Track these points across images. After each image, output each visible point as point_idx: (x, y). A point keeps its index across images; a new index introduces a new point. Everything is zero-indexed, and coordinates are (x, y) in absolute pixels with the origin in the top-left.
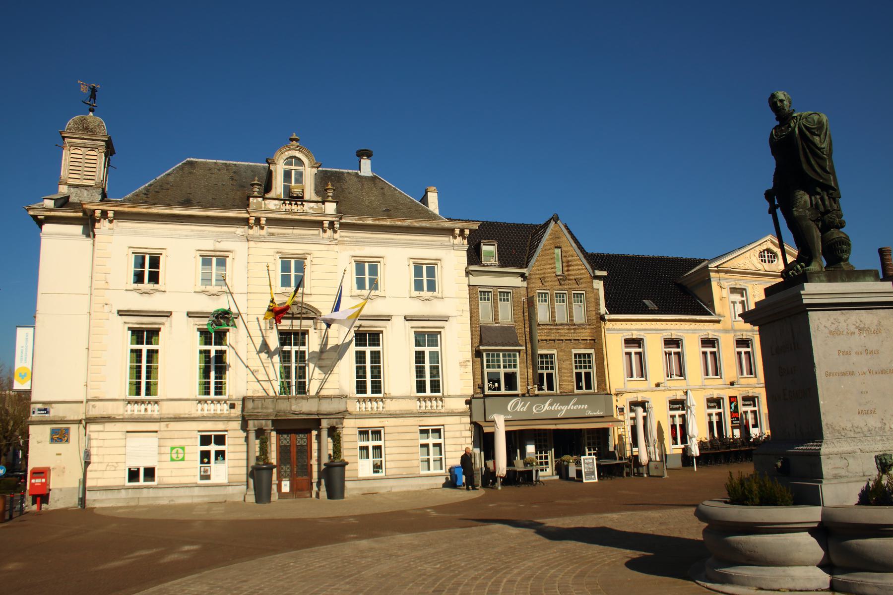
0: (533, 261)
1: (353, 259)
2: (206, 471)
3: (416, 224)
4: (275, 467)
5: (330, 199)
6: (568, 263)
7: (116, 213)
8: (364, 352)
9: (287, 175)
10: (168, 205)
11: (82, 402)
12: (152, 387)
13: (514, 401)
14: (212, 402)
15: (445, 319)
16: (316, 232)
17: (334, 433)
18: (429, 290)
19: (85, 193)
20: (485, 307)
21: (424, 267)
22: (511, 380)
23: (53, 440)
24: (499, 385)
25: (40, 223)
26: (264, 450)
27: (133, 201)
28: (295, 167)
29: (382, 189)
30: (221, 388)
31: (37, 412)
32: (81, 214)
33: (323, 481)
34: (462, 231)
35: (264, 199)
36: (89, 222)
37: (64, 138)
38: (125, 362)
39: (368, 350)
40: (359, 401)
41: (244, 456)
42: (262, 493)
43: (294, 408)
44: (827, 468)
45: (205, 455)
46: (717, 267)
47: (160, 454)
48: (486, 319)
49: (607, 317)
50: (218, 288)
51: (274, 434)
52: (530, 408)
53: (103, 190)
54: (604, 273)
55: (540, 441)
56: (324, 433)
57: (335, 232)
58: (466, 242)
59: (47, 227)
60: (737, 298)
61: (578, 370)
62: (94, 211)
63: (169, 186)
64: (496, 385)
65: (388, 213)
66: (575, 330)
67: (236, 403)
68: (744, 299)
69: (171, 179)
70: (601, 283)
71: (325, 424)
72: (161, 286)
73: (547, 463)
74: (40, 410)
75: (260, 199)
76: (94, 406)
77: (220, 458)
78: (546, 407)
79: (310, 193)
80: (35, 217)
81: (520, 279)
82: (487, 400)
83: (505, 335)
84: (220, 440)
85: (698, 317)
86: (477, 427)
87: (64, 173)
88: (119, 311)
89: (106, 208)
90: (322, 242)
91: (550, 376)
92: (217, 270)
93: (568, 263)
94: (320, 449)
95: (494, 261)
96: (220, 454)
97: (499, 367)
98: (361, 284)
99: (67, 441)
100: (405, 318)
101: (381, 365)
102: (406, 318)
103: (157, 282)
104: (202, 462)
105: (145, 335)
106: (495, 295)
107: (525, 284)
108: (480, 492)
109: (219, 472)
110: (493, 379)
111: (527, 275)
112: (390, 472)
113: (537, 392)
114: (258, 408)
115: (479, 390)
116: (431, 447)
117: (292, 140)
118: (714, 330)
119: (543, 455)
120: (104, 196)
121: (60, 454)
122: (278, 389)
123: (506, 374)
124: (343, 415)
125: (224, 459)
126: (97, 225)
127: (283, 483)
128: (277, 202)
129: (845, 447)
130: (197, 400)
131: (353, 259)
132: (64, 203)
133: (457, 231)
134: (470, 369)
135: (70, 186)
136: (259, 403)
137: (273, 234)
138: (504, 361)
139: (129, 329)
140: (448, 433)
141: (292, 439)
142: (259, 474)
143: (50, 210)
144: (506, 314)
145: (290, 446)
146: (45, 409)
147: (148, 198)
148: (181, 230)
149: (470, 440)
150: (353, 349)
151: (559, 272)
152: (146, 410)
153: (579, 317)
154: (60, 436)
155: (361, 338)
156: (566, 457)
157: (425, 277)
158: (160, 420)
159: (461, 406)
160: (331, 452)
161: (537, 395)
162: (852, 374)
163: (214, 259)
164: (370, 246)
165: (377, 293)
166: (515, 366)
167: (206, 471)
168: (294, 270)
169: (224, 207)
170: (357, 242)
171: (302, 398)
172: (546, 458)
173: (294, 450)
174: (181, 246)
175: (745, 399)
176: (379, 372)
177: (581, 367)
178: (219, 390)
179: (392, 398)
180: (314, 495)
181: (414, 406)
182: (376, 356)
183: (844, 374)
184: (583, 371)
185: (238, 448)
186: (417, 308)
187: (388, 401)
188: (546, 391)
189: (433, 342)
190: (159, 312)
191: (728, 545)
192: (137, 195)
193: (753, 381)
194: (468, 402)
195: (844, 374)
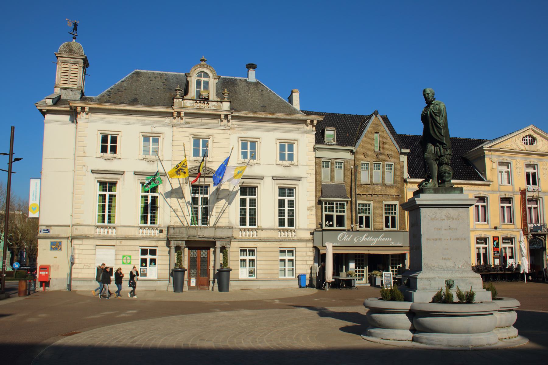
0: (359, 141)
1: (240, 139)
2: (144, 271)
3: (282, 116)
4: (186, 270)
5: (226, 100)
6: (383, 143)
7: (90, 108)
8: (245, 199)
9: (198, 83)
10: (122, 103)
11: (69, 226)
12: (112, 218)
13: (342, 233)
14: (149, 228)
15: (299, 179)
16: (216, 121)
17: (223, 249)
18: (289, 160)
19: (71, 93)
20: (326, 171)
21: (286, 145)
22: (340, 221)
23: (52, 249)
24: (333, 223)
25: (44, 114)
26: (179, 259)
27: (100, 101)
28: (204, 78)
29: (262, 91)
30: (154, 220)
31: (43, 231)
32: (69, 109)
33: (216, 280)
34: (312, 121)
35: (183, 99)
36: (73, 114)
37: (57, 57)
38: (96, 202)
39: (248, 198)
40: (241, 230)
41: (168, 262)
42: (178, 286)
43: (199, 234)
44: (419, 285)
45: (144, 261)
46: (490, 147)
47: (116, 259)
48: (326, 180)
49: (408, 180)
50: (154, 157)
51: (186, 249)
52: (352, 239)
53: (82, 91)
54: (408, 151)
55: (359, 260)
56: (218, 250)
57: (229, 121)
58: (314, 128)
59: (48, 117)
60: (504, 169)
61: (387, 215)
62: (77, 107)
63: (123, 90)
64: (331, 223)
65: (264, 109)
66: (386, 188)
67: (163, 229)
68: (509, 170)
69: (125, 84)
70: (406, 157)
71: (218, 244)
72: (118, 155)
73: (363, 275)
74: (44, 230)
75: (181, 100)
76: (76, 229)
77: (153, 263)
78: (364, 239)
79: (213, 96)
80: (41, 110)
81: (350, 154)
82: (324, 232)
83: (338, 190)
84: (153, 252)
85: (473, 182)
86: (317, 249)
87: (58, 80)
88: (92, 171)
89: (84, 105)
90: (220, 128)
91: (367, 219)
92: (153, 145)
93: (383, 143)
94: (215, 260)
95: (334, 141)
96: (153, 261)
97: (333, 211)
99: (60, 249)
100: (272, 178)
101: (256, 207)
102: (274, 178)
103: (115, 152)
104: (142, 265)
105: (107, 186)
106: (333, 164)
107: (353, 157)
108: (315, 291)
109: (152, 272)
110: (329, 218)
112: (260, 276)
113: (358, 228)
114: (177, 233)
115: (319, 226)
116: (287, 261)
117: (202, 60)
118: (485, 191)
119: (361, 270)
120: (82, 94)
121: (56, 258)
122: (189, 221)
123: (337, 216)
124: (229, 239)
125: (155, 264)
126: (79, 116)
127: (191, 280)
128: (191, 101)
129: (431, 275)
130: (139, 227)
131: (240, 139)
132: (58, 101)
133: (309, 122)
134: (314, 212)
135: (61, 88)
136: (177, 230)
137: (188, 123)
138: (337, 208)
139: (98, 181)
140: (297, 253)
141: (198, 254)
142: (176, 274)
143: (50, 106)
144: (340, 177)
145: (196, 257)
146: (47, 230)
147: (111, 98)
148: (130, 119)
149: (312, 258)
150: (238, 197)
151: (377, 149)
152: (108, 232)
153: (389, 178)
154: (56, 246)
155: (244, 190)
156: (375, 272)
157: (287, 151)
158: (116, 239)
159: (307, 235)
160: (222, 262)
161: (358, 231)
162: (441, 239)
163: (151, 138)
164: (252, 130)
165: (255, 161)
166: (344, 211)
167: (144, 271)
168: (201, 145)
169: (159, 105)
170: (243, 128)
171: (205, 228)
172: (363, 272)
173: (199, 260)
174: (131, 130)
175: (505, 239)
176: (255, 212)
177: (389, 213)
178: (153, 221)
180: (211, 289)
182: (253, 202)
183: (437, 239)
184: (390, 216)
185: (164, 258)
186: (281, 172)
187: (260, 231)
188: (364, 228)
189: (291, 194)
190: (116, 171)
191: (371, 317)
192: (103, 96)
193: (512, 226)
194: (312, 234)
195: (437, 239)
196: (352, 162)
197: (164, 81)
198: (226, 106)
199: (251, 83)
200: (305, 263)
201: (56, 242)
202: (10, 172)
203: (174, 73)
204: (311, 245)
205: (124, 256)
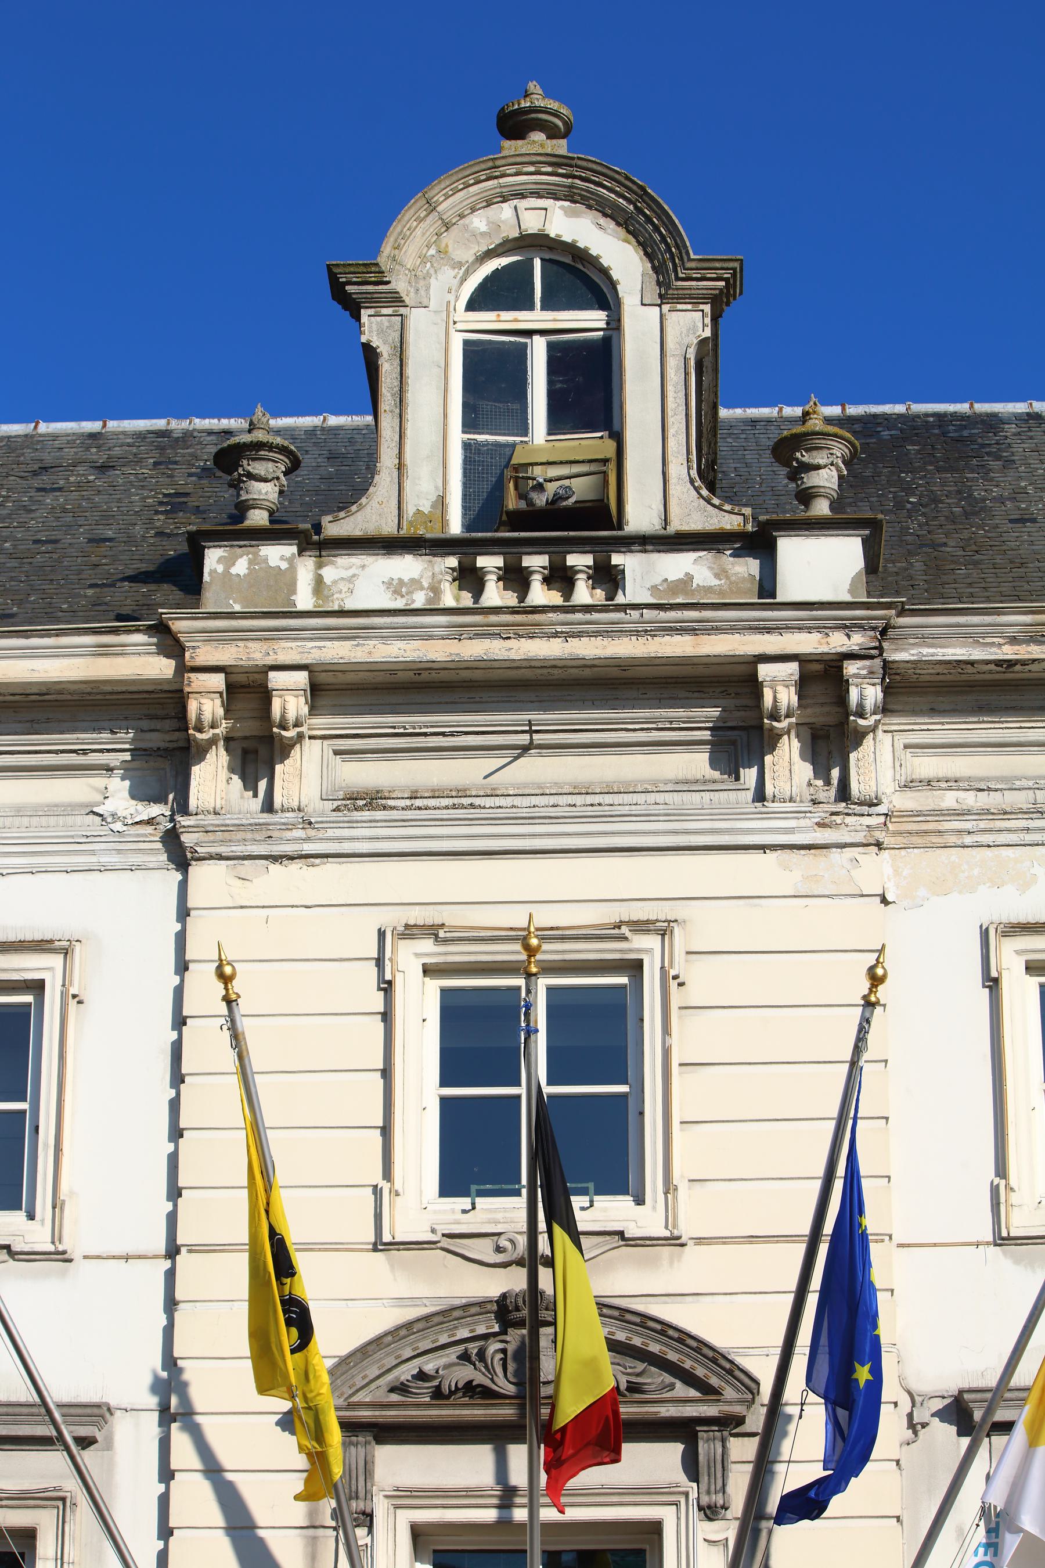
35: (318, 544)
75: (277, 554)
128: (407, 566)
137: (371, 799)
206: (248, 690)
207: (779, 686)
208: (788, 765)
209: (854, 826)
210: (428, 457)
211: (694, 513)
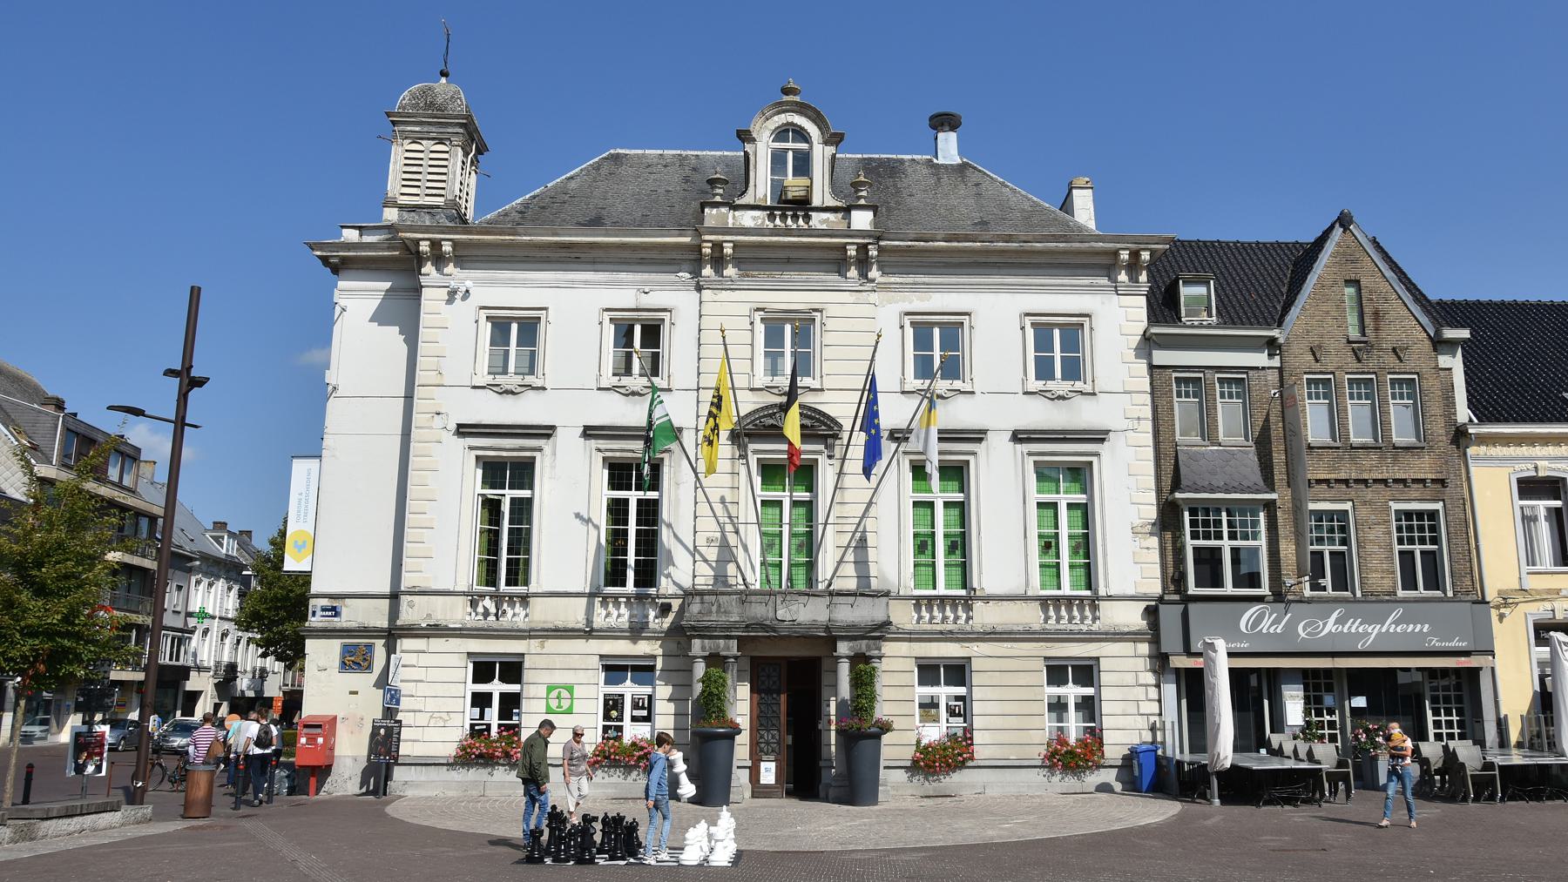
0: (1295, 311)
1: (907, 321)
9: (778, 159)
13: (1256, 608)
15: (1098, 436)
23: (345, 666)
25: (336, 270)
38: (470, 522)
52: (1291, 627)
54: (1465, 334)
61: (1406, 547)
62: (417, 242)
66: (1395, 459)
71: (843, 648)
75: (724, 210)
76: (411, 605)
78: (1331, 626)
82: (1192, 607)
87: (394, 187)
93: (1377, 315)
97: (1219, 536)
98: (924, 368)
102: (1018, 437)
104: (607, 717)
111: (1281, 341)
113: (1307, 593)
123: (1235, 551)
124: (881, 631)
135: (401, 207)
146: (334, 609)
151: (1354, 333)
157: (1060, 350)
161: (1310, 601)
177: (1411, 541)
179: (987, 599)
181: (1031, 616)
192: (506, 215)
196: (1273, 377)
197: (688, 172)
198: (862, 220)
199: (946, 167)
200: (1132, 708)
201: (358, 645)
202: (180, 424)
203: (719, 153)
204: (1144, 648)
205: (550, 688)
206: (718, 246)
207: (852, 252)
208: (853, 273)
209: (869, 286)
210: (762, 186)
211: (830, 202)
